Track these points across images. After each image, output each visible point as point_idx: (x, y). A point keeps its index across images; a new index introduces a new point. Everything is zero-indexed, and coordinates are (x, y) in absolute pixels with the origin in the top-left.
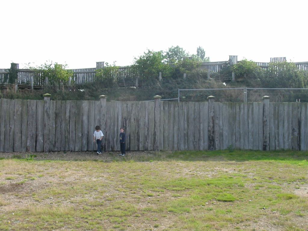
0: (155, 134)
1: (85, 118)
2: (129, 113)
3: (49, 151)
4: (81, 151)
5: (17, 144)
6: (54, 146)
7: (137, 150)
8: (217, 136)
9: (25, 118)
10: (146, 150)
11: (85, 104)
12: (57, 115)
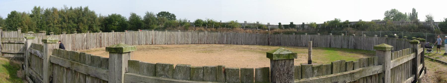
0: (317, 43)
1: (302, 39)
2: (312, 38)
3: (294, 46)
4: (301, 46)
5: (287, 44)
6: (295, 45)
7: (304, 46)
8: (331, 44)
9: (289, 38)
10: (315, 47)
11: (302, 36)
12: (295, 38)
